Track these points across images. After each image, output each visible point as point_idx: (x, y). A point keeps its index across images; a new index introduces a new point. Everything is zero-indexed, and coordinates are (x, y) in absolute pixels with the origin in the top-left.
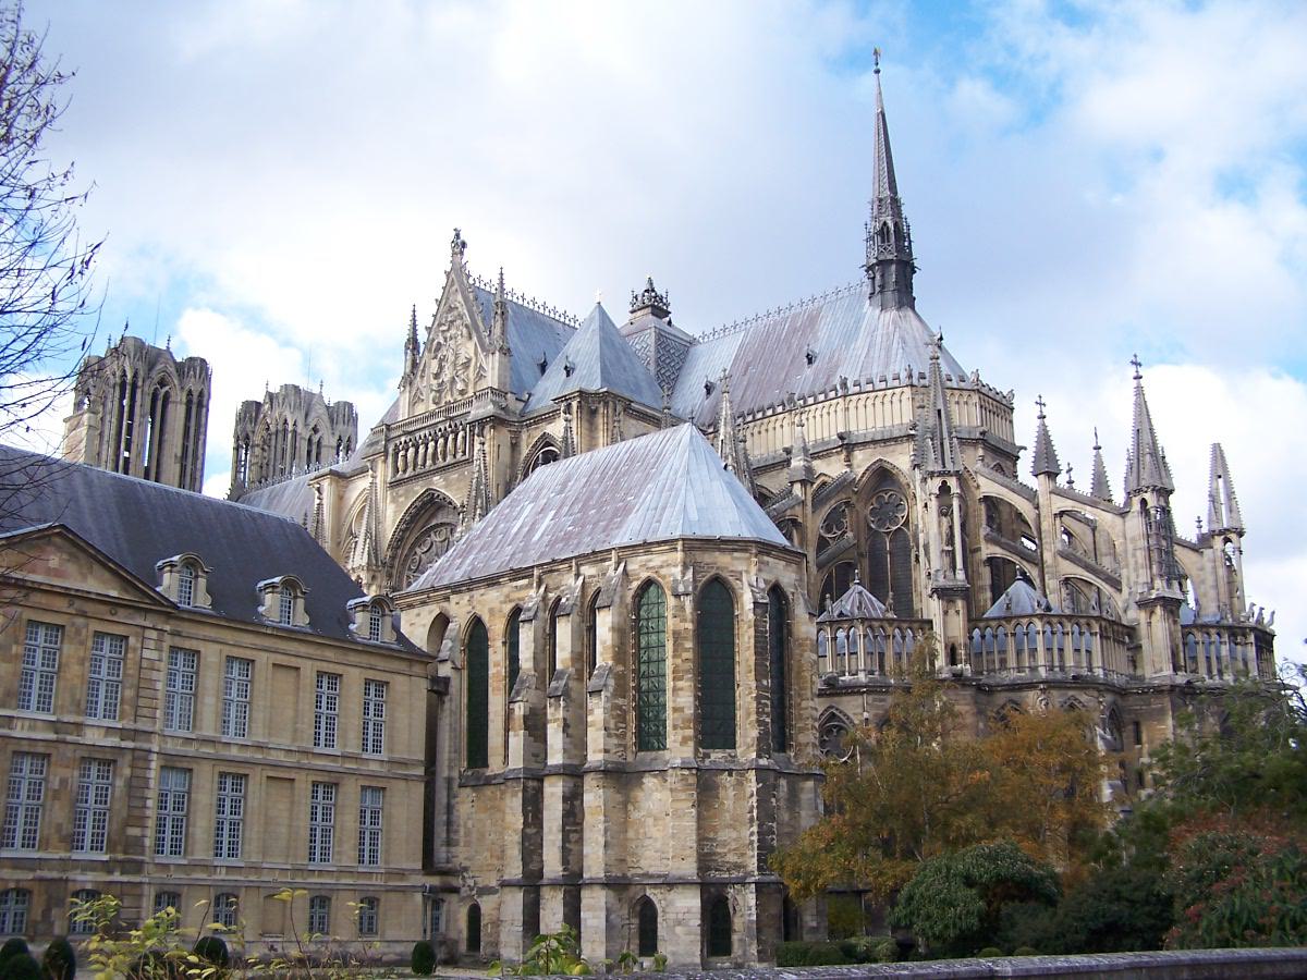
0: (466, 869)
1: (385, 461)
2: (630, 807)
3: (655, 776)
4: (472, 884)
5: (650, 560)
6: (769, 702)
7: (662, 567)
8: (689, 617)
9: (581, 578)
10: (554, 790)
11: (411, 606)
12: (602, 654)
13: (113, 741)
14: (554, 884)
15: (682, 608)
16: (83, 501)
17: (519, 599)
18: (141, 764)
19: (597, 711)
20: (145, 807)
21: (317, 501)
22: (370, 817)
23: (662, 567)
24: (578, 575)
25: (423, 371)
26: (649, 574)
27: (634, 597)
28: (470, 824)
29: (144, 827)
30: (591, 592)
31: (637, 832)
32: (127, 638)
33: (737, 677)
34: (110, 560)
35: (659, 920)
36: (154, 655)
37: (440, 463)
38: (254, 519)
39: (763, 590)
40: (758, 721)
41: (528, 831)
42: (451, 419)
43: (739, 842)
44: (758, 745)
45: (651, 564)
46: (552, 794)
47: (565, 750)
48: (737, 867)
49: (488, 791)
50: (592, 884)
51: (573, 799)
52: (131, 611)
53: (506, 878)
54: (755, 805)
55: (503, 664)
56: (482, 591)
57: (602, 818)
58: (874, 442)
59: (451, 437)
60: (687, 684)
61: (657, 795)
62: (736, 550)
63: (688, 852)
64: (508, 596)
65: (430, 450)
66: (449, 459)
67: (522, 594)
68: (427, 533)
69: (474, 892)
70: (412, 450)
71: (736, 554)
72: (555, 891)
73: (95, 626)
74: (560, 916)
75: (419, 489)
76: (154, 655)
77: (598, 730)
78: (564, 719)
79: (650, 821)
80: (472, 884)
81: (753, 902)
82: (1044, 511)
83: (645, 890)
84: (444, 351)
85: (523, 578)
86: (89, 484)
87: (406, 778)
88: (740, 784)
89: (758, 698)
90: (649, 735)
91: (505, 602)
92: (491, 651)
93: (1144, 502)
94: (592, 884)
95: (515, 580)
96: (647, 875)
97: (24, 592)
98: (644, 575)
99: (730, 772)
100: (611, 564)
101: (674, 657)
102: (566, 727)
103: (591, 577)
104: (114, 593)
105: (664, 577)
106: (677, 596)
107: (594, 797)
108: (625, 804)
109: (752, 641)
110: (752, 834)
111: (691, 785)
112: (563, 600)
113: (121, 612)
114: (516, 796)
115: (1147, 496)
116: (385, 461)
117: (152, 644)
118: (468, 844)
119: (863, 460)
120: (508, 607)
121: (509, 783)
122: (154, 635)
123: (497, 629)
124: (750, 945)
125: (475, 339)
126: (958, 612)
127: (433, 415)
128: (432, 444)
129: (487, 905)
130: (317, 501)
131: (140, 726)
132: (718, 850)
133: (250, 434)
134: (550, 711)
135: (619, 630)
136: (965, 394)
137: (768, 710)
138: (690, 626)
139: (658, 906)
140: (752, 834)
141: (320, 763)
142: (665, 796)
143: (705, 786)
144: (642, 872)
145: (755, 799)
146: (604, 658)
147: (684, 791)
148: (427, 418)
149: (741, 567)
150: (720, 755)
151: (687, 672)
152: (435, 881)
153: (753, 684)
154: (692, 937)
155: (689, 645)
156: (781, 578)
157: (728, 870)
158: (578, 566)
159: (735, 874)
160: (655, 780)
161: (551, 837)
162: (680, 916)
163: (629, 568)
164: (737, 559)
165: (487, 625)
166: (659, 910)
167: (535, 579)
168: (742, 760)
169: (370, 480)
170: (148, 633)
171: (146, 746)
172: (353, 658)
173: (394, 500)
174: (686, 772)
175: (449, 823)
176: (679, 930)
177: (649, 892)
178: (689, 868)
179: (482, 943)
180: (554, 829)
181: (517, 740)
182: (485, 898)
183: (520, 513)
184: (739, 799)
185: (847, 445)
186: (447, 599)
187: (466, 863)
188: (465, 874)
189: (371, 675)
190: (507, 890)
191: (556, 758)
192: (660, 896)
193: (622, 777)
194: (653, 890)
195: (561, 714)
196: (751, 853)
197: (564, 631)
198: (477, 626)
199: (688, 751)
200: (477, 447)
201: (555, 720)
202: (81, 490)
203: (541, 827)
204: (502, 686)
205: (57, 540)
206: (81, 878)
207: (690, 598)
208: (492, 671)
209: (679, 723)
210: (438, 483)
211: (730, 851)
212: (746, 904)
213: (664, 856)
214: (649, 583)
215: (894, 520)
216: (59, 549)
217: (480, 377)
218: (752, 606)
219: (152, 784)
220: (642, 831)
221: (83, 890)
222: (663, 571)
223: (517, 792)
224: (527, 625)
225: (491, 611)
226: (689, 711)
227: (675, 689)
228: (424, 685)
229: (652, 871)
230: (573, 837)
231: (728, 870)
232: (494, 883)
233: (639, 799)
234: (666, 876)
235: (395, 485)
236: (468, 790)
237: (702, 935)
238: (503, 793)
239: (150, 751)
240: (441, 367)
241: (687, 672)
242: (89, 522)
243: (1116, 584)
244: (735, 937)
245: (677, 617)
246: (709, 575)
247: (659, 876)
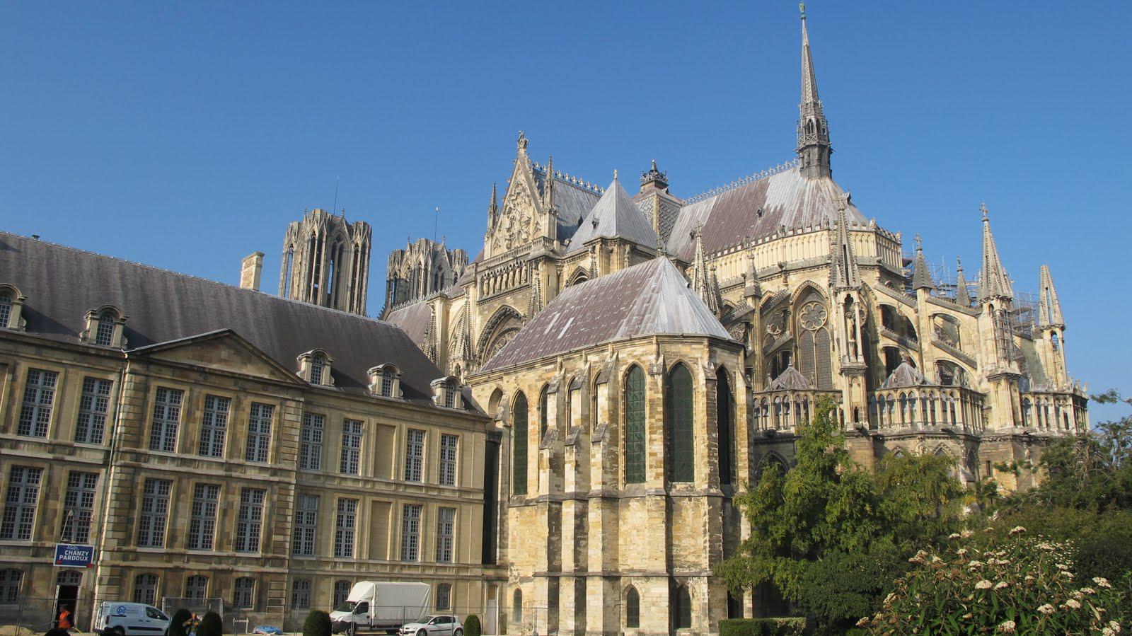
0: (512, 564)
1: (475, 287)
2: (621, 522)
3: (638, 501)
6: (717, 449)
7: (642, 355)
8: (660, 389)
9: (588, 364)
10: (569, 510)
11: (478, 384)
12: (601, 416)
13: (265, 476)
14: (568, 576)
15: (656, 384)
16: (251, 316)
17: (548, 378)
18: (283, 492)
19: (597, 455)
20: (286, 521)
21: (432, 315)
22: (444, 529)
23: (642, 355)
24: (586, 361)
25: (500, 227)
27: (623, 377)
29: (285, 535)
30: (594, 373)
31: (625, 540)
32: (274, 406)
33: (695, 432)
34: (263, 354)
35: (641, 601)
36: (293, 418)
37: (511, 287)
38: (368, 326)
39: (712, 370)
40: (709, 462)
41: (553, 538)
42: (517, 258)
43: (696, 545)
44: (709, 479)
45: (635, 353)
46: (567, 513)
47: (576, 483)
48: (696, 565)
49: (527, 510)
50: (594, 575)
51: (581, 517)
52: (278, 388)
54: (707, 521)
55: (537, 423)
56: (524, 373)
57: (601, 530)
58: (803, 269)
59: (518, 270)
60: (659, 436)
61: (639, 514)
62: (692, 343)
64: (540, 376)
65: (505, 279)
66: (517, 285)
67: (549, 375)
68: (502, 334)
69: (518, 580)
70: (492, 280)
71: (694, 346)
73: (251, 399)
74: (572, 598)
75: (497, 305)
76: (293, 418)
77: (598, 468)
78: (576, 462)
79: (634, 532)
81: (706, 590)
82: (921, 314)
84: (513, 213)
85: (551, 364)
86: (254, 303)
87: (471, 502)
88: (697, 506)
89: (709, 447)
90: (635, 473)
91: (537, 381)
92: (529, 414)
93: (991, 306)
94: (594, 575)
95: (545, 365)
96: (632, 570)
97: (203, 375)
98: (631, 361)
99: (690, 498)
100: (608, 354)
101: (650, 417)
102: (577, 466)
103: (595, 362)
104: (266, 376)
105: (644, 362)
106: (652, 375)
107: (595, 514)
108: (617, 520)
109: (705, 405)
111: (662, 507)
112: (577, 379)
113: (270, 387)
114: (544, 514)
115: (993, 302)
116: (475, 287)
117: (292, 411)
118: (514, 547)
119: (795, 283)
120: (540, 384)
121: (540, 505)
122: (293, 404)
123: (533, 399)
124: (704, 620)
125: (533, 205)
126: (859, 385)
127: (506, 256)
128: (505, 275)
129: (526, 589)
130: (432, 315)
131: (282, 466)
132: (682, 553)
133: (398, 272)
134: (567, 455)
135: (613, 399)
136: (866, 234)
137: (716, 454)
138: (661, 396)
140: (705, 542)
141: (410, 491)
142: (644, 515)
143: (670, 509)
145: (707, 516)
146: (603, 418)
148: (502, 258)
149: (698, 355)
150: (683, 486)
151: (658, 428)
152: (490, 573)
153: (706, 436)
154: (663, 615)
155: (660, 409)
156: (726, 363)
157: (689, 567)
158: (586, 355)
159: (693, 570)
162: (654, 599)
163: (620, 356)
164: (695, 349)
165: (527, 397)
166: (641, 595)
167: (558, 364)
168: (698, 489)
169: (466, 300)
170: (289, 403)
171: (287, 480)
172: (433, 419)
173: (481, 313)
174: (658, 498)
175: (502, 532)
176: (653, 609)
177: (634, 582)
178: (661, 566)
179: (523, 616)
180: (569, 537)
181: (545, 475)
183: (552, 319)
184: (696, 519)
185: (784, 271)
186: (501, 378)
189: (446, 431)
190: (537, 579)
191: (570, 488)
193: (611, 500)
195: (573, 458)
197: (577, 399)
198: (521, 399)
199: (660, 484)
200: (534, 276)
201: (570, 462)
202: (249, 309)
203: (560, 535)
204: (537, 437)
205: (227, 340)
206: (241, 569)
207: (661, 376)
208: (530, 427)
209: (654, 464)
210: (509, 301)
211: (689, 554)
212: (700, 592)
214: (633, 367)
215: (817, 322)
216: (229, 346)
217: (537, 230)
218: (705, 382)
219: (291, 505)
220: (629, 539)
221: (244, 577)
222: (643, 358)
224: (552, 396)
225: (529, 386)
226: (661, 456)
227: (651, 440)
228: (483, 438)
230: (583, 543)
231: (689, 567)
234: (645, 571)
235: (480, 303)
237: (670, 613)
238: (536, 511)
239: (290, 484)
240: (512, 224)
241: (658, 428)
242: (253, 328)
243: (973, 364)
244: (693, 615)
245: (653, 390)
246: (674, 361)
247: (640, 571)
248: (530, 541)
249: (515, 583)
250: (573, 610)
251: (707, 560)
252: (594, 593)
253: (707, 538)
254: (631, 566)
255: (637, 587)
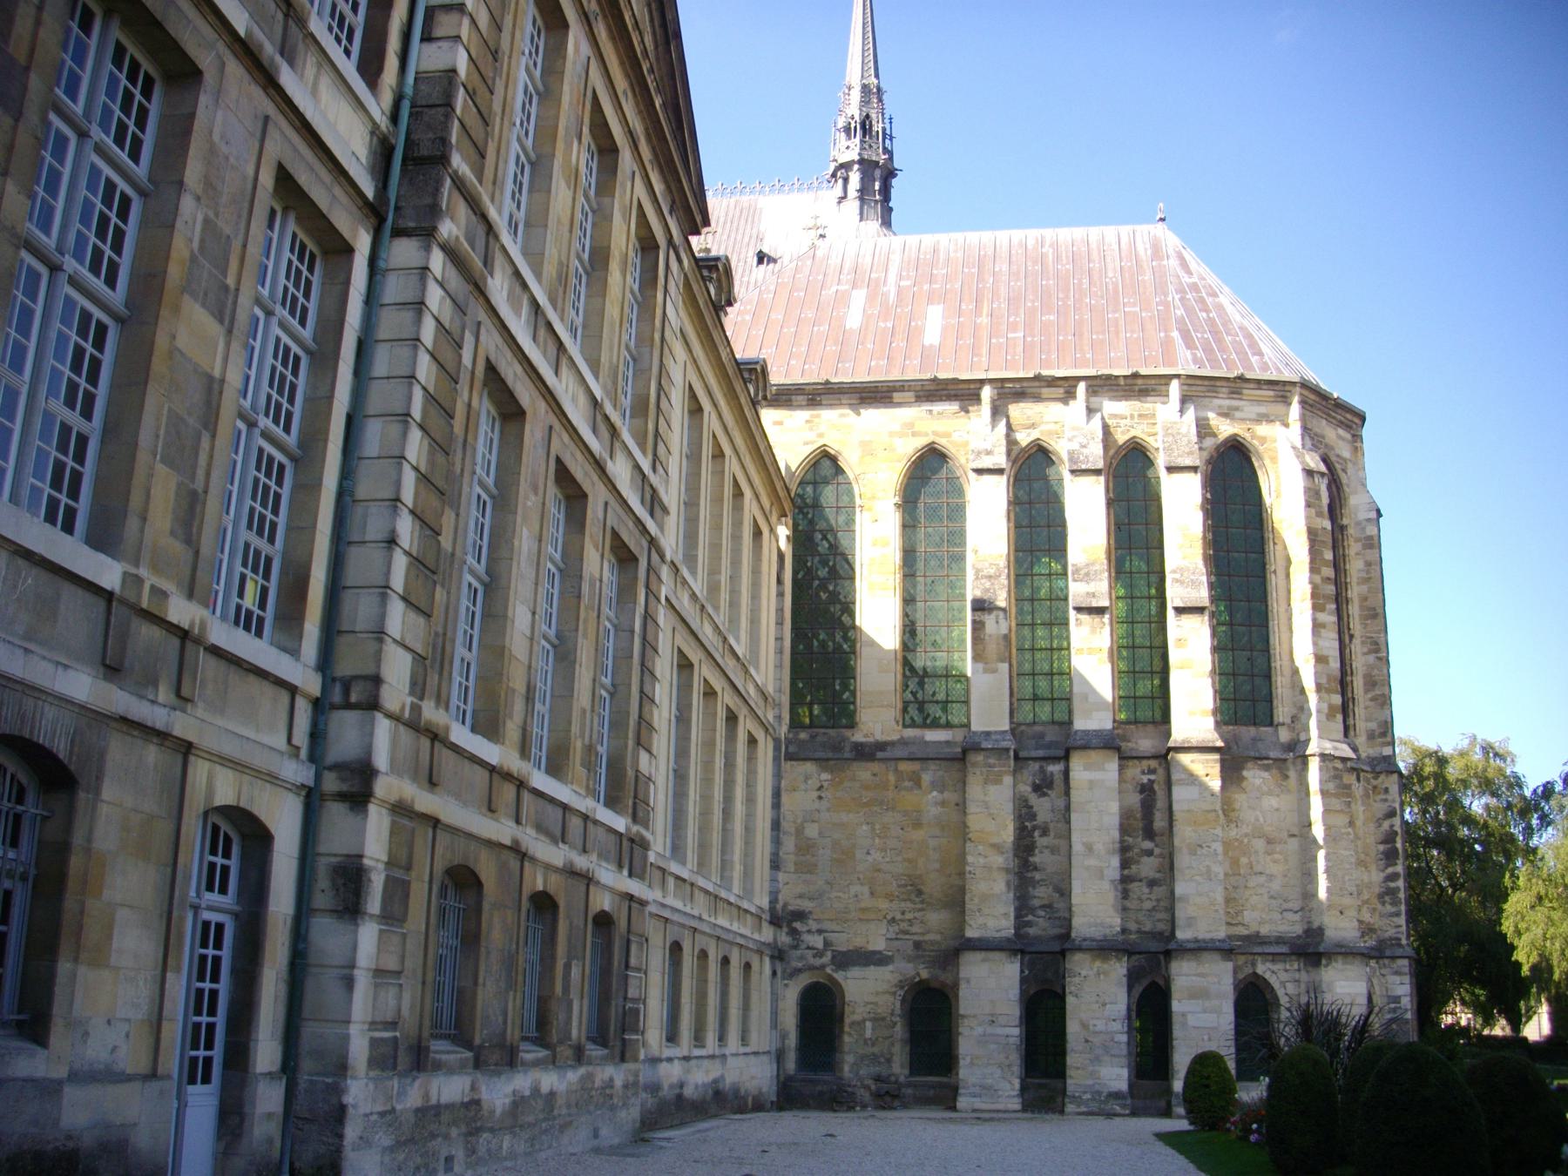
0: (800, 915)
3: (1267, 768)
4: (820, 945)
5: (1237, 409)
14: (1104, 949)
15: (1318, 493)
17: (935, 433)
24: (1091, 411)
26: (1236, 431)
28: (812, 831)
46: (1092, 784)
50: (1199, 949)
53: (969, 933)
61: (1271, 802)
63: (1347, 901)
72: (1105, 959)
79: (1259, 844)
80: (820, 945)
83: (1254, 965)
91: (902, 435)
94: (1199, 949)
103: (1114, 416)
105: (1263, 440)
110: (1393, 877)
114: (998, 781)
120: (910, 447)
139: (1280, 993)
144: (1246, 932)
147: (1336, 795)
160: (1266, 775)
161: (1092, 862)
177: (1262, 969)
180: (1099, 847)
182: (855, 972)
187: (806, 905)
188: (797, 925)
192: (1284, 976)
194: (1269, 965)
196: (1389, 908)
201: (1091, 651)
213: (1286, 906)
220: (1244, 860)
223: (1000, 774)
229: (1264, 931)
232: (878, 944)
233: (1237, 806)
236: (809, 767)
248: (876, 855)
249: (812, 968)
250: (1124, 1038)
251: (1402, 920)
252: (1199, 994)
253: (1399, 868)
254: (1254, 928)
255: (1273, 980)
